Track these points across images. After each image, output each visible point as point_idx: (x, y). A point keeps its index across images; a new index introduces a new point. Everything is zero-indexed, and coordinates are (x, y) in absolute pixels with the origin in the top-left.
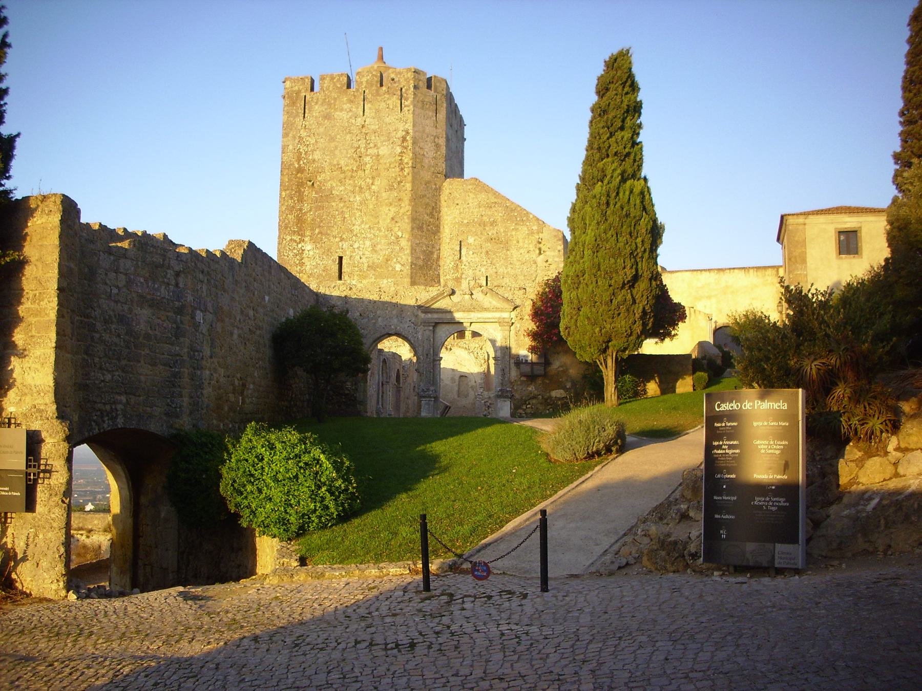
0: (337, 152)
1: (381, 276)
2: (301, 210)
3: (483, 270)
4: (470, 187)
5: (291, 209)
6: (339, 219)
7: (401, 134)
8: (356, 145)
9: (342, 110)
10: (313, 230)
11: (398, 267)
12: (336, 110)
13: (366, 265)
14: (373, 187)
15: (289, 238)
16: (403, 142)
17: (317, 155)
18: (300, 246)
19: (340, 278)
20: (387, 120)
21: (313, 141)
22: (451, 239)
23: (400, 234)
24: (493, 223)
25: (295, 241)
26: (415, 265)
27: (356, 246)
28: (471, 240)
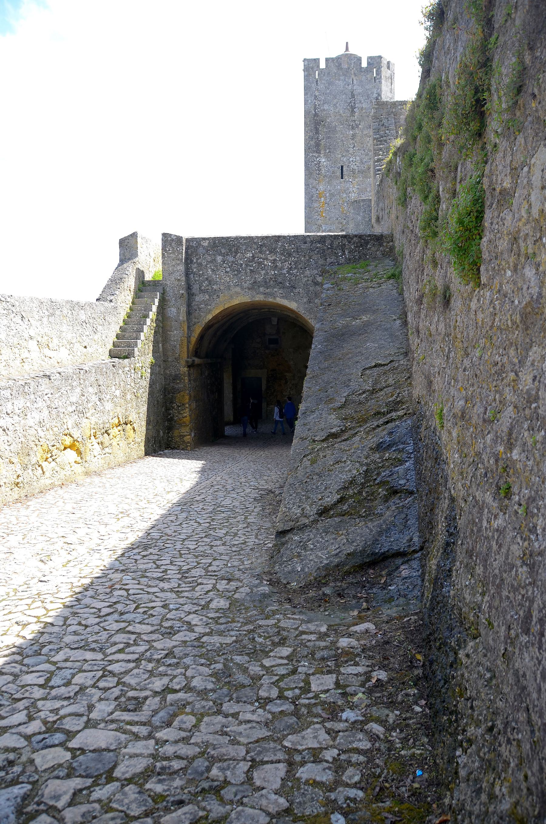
0: (338, 105)
1: (366, 177)
2: (318, 138)
5: (311, 138)
6: (340, 144)
7: (375, 95)
9: (339, 80)
10: (325, 150)
15: (311, 155)
17: (326, 107)
19: (342, 178)
20: (367, 87)
27: (351, 159)
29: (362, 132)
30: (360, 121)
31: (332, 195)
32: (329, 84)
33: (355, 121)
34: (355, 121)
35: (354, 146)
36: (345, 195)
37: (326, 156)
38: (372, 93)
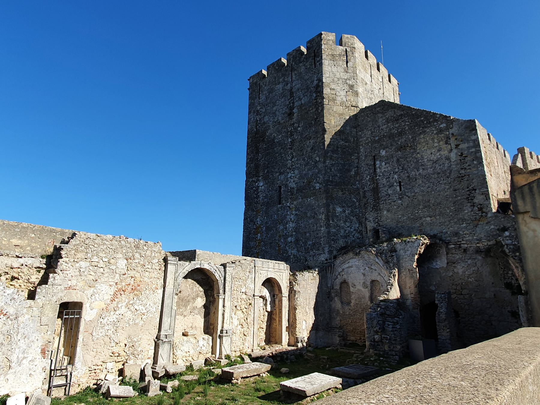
0: (277, 113)
2: (258, 158)
3: (396, 176)
4: (378, 109)
7: (316, 82)
8: (288, 103)
11: (317, 186)
12: (276, 85)
13: (296, 189)
16: (317, 89)
18: (257, 184)
20: (306, 77)
21: (264, 110)
22: (366, 156)
23: (317, 159)
24: (401, 134)
25: (254, 181)
26: (332, 182)
28: (383, 153)
29: (301, 134)
30: (299, 122)
31: (268, 229)
32: (269, 93)
33: (293, 124)
34: (293, 124)
35: (293, 157)
36: (281, 227)
37: (265, 178)
38: (312, 82)
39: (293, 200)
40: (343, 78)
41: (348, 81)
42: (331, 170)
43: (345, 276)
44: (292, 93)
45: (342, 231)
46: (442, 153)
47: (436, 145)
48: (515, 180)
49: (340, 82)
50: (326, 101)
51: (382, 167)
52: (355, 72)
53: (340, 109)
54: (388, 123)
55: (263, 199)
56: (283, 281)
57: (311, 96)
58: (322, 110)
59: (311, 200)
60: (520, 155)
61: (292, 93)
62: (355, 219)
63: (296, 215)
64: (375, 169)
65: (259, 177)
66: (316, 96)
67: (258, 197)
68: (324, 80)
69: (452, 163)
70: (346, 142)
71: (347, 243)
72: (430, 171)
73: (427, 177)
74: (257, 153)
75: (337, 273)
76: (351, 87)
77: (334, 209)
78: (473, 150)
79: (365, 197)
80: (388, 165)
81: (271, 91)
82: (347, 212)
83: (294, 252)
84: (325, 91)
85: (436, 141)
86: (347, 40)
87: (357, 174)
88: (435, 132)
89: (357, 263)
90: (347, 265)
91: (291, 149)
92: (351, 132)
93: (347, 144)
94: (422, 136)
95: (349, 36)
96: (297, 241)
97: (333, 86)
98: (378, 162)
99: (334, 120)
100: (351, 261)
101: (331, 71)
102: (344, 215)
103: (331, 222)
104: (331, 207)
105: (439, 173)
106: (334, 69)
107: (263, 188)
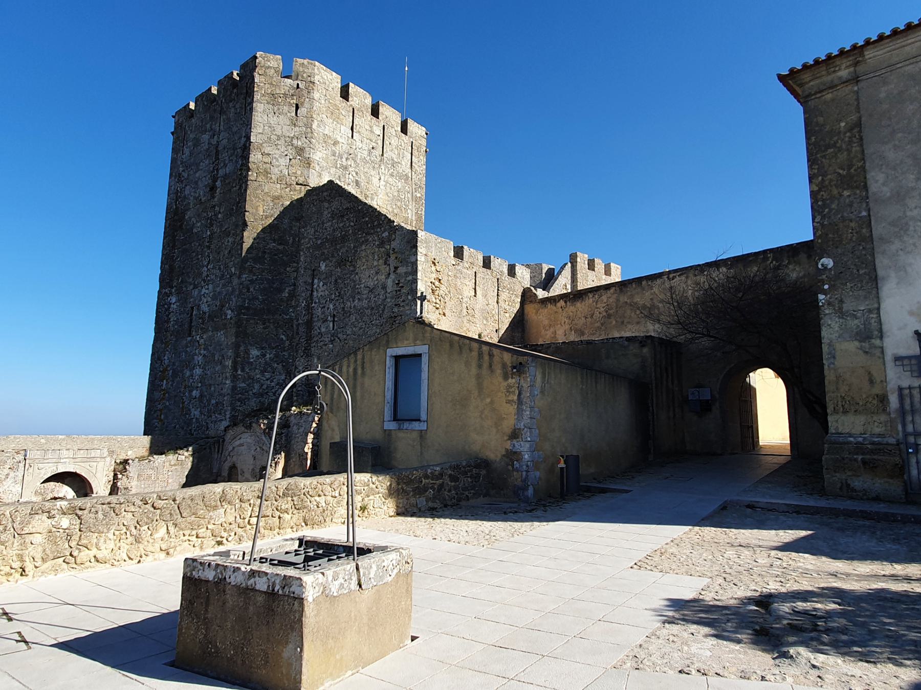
0: (199, 183)
1: (217, 329)
3: (331, 306)
4: (325, 194)
14: (220, 216)
20: (235, 129)
22: (305, 268)
24: (344, 239)
26: (248, 308)
28: (323, 267)
29: (221, 226)
30: (220, 205)
31: (175, 374)
34: (214, 207)
37: (179, 292)
38: (240, 138)
39: (205, 331)
40: (288, 134)
41: (295, 142)
42: (248, 289)
43: (234, 459)
44: (217, 152)
45: (257, 386)
46: (379, 277)
47: (375, 263)
48: (526, 311)
49: (281, 142)
50: (252, 175)
51: (321, 289)
52: (309, 126)
53: (276, 189)
54: (333, 218)
55: (173, 326)
56: (98, 475)
57: (237, 162)
58: (246, 190)
59: (220, 336)
60: (569, 264)
61: (217, 152)
62: (280, 366)
63: (204, 356)
64: (312, 291)
65: (172, 288)
66: (242, 165)
67: (168, 321)
68: (253, 139)
69: (388, 295)
70: (281, 244)
71: (263, 404)
72: (365, 303)
73: (360, 312)
74: (174, 247)
75: (227, 453)
76: (300, 151)
77: (247, 352)
78: (410, 278)
79: (298, 333)
80: (325, 287)
81: (197, 142)
82: (268, 356)
83: (197, 413)
84: (252, 158)
85: (376, 257)
86: (301, 69)
87: (292, 295)
88: (377, 243)
89: (248, 440)
90: (238, 443)
91: (209, 247)
92: (291, 228)
93: (281, 247)
94: (364, 247)
95: (306, 61)
96: (202, 396)
97: (267, 150)
98: (316, 281)
99: (262, 207)
100: (242, 436)
101: (266, 122)
102: (263, 361)
103: (239, 372)
104: (242, 348)
105: (373, 308)
106: (273, 120)
107: (175, 306)
